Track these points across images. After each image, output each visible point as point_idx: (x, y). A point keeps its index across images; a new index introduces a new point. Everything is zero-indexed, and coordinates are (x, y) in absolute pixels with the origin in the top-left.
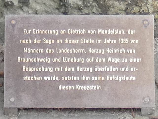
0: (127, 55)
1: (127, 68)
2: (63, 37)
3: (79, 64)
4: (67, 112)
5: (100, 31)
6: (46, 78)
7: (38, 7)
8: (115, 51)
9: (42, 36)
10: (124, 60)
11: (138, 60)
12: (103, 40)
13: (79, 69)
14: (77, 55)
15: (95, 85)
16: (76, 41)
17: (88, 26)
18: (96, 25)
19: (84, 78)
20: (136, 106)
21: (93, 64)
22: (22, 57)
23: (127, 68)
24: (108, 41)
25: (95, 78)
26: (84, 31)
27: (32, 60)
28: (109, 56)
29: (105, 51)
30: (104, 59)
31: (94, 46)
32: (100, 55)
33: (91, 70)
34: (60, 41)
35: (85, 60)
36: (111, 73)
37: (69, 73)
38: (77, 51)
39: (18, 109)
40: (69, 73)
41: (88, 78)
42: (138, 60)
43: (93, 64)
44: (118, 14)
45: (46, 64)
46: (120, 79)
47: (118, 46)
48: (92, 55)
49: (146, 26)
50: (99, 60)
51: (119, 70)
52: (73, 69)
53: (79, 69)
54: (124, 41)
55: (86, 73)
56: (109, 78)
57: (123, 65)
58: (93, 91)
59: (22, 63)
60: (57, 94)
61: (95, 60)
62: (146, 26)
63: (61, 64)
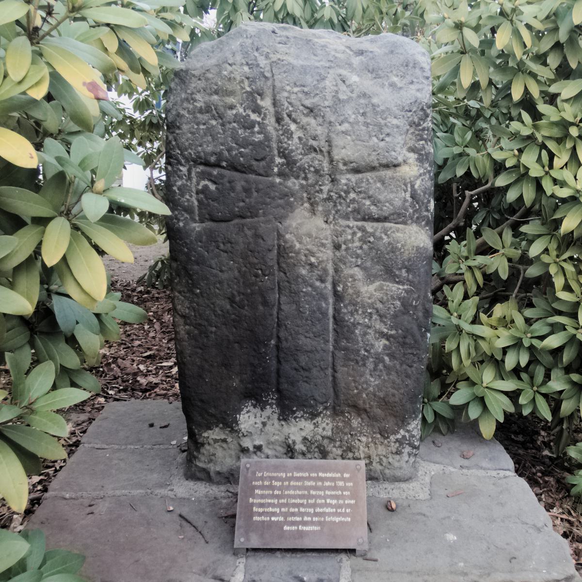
0: (342, 497)
1: (344, 510)
2: (289, 479)
3: (302, 505)
4: (290, 554)
5: (320, 474)
6: (273, 519)
7: (270, 452)
8: (333, 493)
9: (271, 479)
10: (341, 502)
11: (353, 502)
12: (323, 483)
13: (302, 510)
14: (302, 497)
15: (315, 526)
16: (299, 484)
17: (311, 469)
18: (317, 469)
19: (306, 519)
20: (351, 547)
21: (314, 506)
22: (254, 498)
23: (344, 510)
24: (327, 484)
25: (315, 519)
26: (307, 474)
27: (262, 501)
28: (328, 498)
29: (325, 493)
30: (323, 501)
31: (316, 488)
32: (320, 497)
33: (311, 510)
34: (286, 483)
35: (307, 501)
36: (330, 514)
37: (293, 514)
38: (300, 493)
39: (247, 549)
40: (293, 514)
41: (309, 519)
42: (353, 502)
43: (314, 506)
44: (335, 459)
45: (273, 505)
46: (337, 519)
47: (335, 488)
48: (313, 497)
49: (359, 470)
50: (319, 501)
51: (336, 511)
52: (296, 510)
53: (302, 510)
54: (341, 484)
55: (308, 514)
56: (328, 519)
57: (340, 506)
58: (314, 532)
59: (253, 505)
60: (282, 534)
61: (315, 501)
62: (359, 470)
63: (286, 505)
